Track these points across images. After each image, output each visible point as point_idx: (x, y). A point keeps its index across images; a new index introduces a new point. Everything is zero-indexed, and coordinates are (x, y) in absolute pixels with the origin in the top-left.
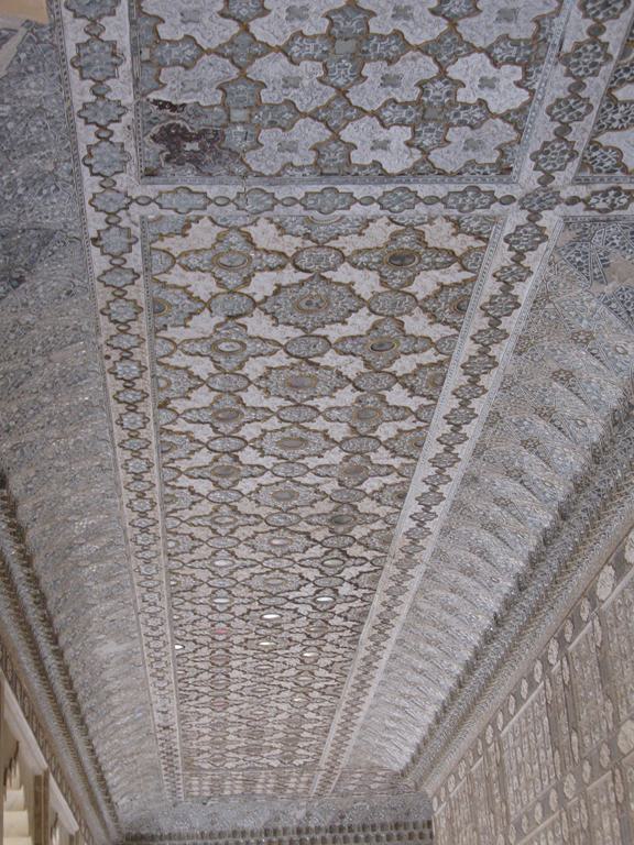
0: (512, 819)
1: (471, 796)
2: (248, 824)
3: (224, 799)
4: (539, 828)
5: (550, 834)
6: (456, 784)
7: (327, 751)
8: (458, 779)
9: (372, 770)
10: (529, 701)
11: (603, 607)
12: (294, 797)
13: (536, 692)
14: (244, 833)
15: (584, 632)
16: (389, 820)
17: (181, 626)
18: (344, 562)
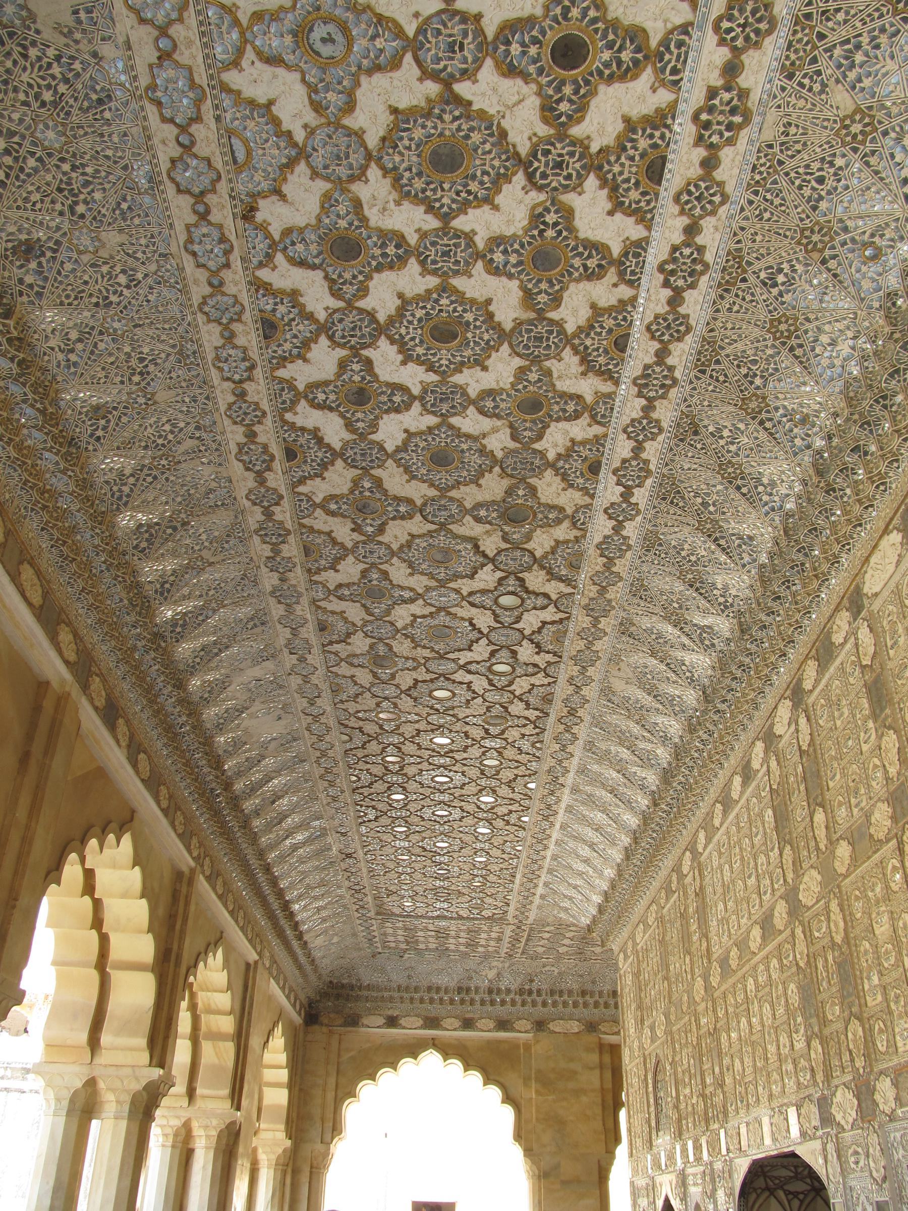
0: (715, 956)
1: (662, 942)
2: (443, 980)
3: (419, 952)
4: (757, 959)
5: (774, 962)
6: (645, 932)
7: (514, 899)
8: (647, 926)
9: (561, 927)
10: (743, 801)
11: (876, 605)
12: (486, 956)
13: (754, 784)
14: (438, 990)
15: (838, 662)
16: (575, 986)
17: (342, 702)
18: (523, 600)
